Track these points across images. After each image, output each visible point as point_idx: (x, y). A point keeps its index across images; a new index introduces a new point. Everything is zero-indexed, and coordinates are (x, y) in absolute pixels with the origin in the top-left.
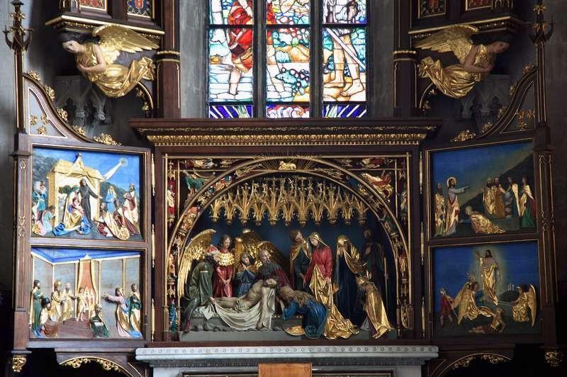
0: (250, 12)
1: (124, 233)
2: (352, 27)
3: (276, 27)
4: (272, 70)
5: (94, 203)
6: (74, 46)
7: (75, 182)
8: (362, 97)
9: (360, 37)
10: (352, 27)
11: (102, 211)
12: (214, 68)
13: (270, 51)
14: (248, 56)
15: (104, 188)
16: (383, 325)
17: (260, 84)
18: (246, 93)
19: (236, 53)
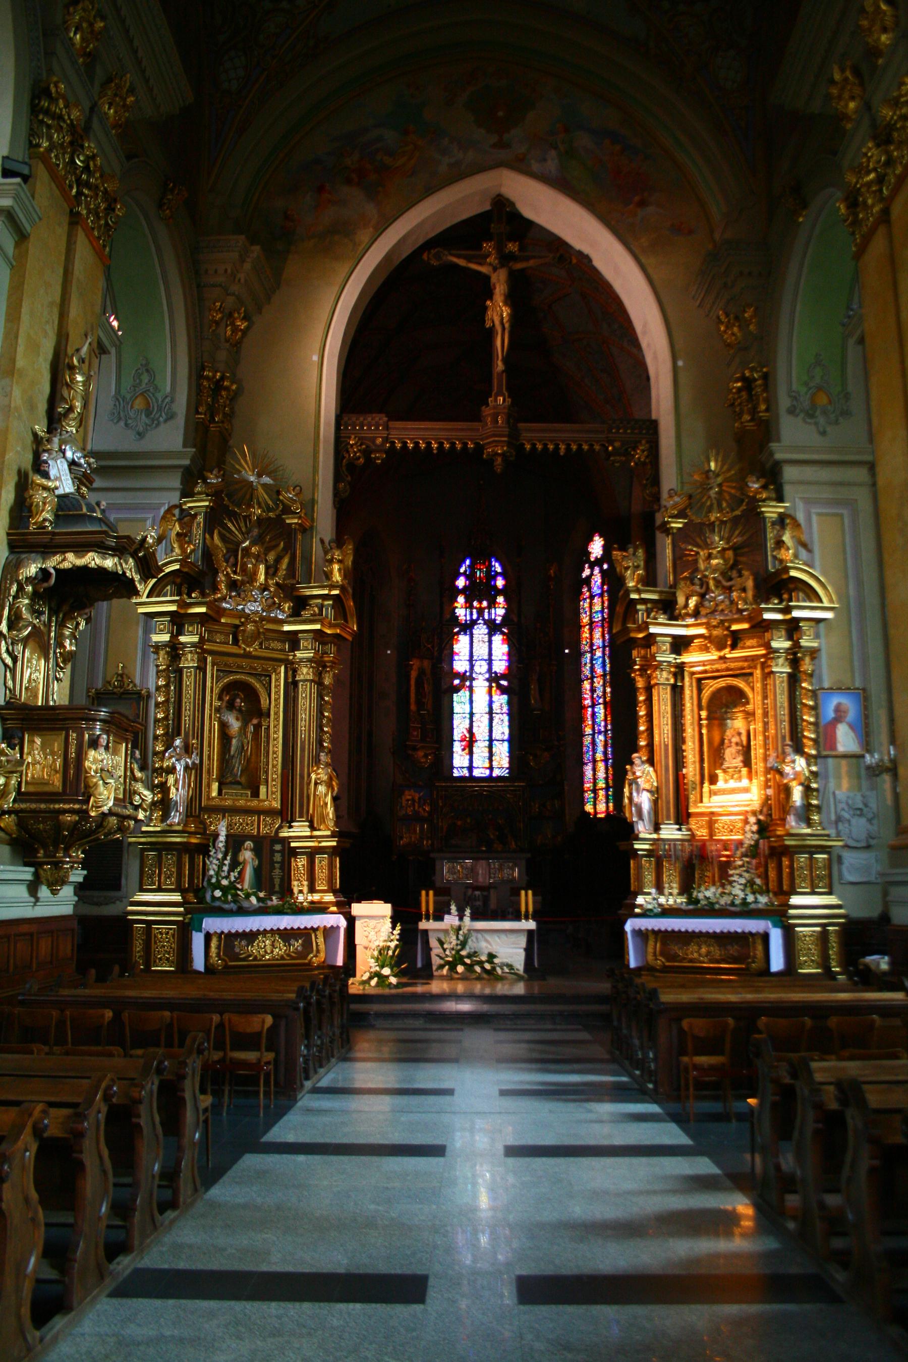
0: (467, 735)
1: (426, 814)
2: (503, 741)
5: (416, 805)
6: (410, 752)
7: (409, 797)
8: (507, 765)
9: (506, 744)
10: (503, 741)
11: (419, 807)
13: (474, 749)
14: (467, 751)
15: (419, 798)
16: (513, 845)
18: (466, 764)
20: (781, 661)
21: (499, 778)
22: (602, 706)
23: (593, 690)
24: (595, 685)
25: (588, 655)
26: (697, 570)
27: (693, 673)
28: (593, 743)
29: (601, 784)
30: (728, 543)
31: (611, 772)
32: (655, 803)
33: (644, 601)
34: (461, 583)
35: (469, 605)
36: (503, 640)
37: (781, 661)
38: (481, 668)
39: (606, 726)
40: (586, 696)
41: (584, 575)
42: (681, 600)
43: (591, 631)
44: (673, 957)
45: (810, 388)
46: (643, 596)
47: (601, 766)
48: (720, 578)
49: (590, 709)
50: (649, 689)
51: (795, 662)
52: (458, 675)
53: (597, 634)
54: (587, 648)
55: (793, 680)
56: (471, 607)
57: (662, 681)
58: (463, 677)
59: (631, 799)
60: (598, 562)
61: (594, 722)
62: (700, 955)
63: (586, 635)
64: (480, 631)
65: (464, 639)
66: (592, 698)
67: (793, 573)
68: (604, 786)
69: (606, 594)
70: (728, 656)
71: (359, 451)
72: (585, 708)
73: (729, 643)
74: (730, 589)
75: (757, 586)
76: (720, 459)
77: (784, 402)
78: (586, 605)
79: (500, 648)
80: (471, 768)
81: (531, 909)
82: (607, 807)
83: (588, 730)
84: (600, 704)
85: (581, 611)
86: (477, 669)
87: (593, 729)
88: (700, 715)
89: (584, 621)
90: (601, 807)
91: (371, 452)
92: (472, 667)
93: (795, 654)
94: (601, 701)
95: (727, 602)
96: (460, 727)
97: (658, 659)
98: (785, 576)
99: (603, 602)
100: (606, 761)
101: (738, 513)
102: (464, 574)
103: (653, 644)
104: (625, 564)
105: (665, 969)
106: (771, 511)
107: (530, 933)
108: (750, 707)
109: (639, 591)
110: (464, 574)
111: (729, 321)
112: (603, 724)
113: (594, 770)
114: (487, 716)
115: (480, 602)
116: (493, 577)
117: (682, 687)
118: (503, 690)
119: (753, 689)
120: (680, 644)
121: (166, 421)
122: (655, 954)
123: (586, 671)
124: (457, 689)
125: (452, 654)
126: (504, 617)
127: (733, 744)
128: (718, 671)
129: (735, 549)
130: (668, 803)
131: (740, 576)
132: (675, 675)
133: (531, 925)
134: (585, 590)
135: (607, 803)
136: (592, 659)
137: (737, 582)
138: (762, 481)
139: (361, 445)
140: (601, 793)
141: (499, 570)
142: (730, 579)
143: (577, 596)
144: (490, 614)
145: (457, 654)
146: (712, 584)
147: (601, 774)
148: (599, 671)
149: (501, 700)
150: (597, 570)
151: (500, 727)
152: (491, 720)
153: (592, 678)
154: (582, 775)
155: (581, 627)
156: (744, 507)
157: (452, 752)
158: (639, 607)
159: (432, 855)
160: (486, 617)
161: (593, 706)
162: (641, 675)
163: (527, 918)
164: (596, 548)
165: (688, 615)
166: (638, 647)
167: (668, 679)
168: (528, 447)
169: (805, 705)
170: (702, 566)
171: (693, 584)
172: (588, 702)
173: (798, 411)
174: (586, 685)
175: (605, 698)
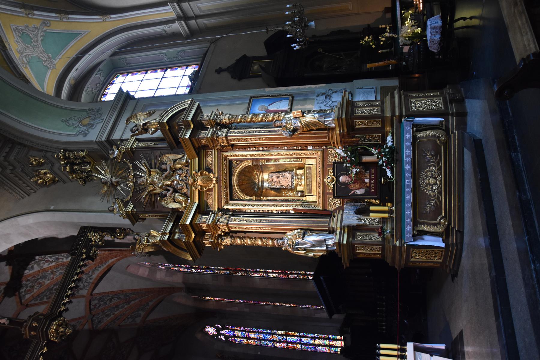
22: (288, 337)
23: (279, 341)
24: (277, 340)
25: (262, 342)
28: (306, 344)
29: (327, 342)
31: (320, 336)
32: (311, 231)
33: (172, 233)
37: (220, 133)
39: (297, 336)
40: (282, 346)
41: (224, 339)
43: (250, 339)
44: (438, 208)
45: (78, 125)
46: (168, 232)
47: (318, 342)
49: (289, 345)
53: (253, 335)
54: (259, 342)
57: (225, 221)
59: (307, 250)
60: (218, 330)
62: (435, 184)
63: (252, 342)
66: (283, 342)
68: (328, 341)
69: (233, 328)
70: (216, 176)
72: (288, 347)
73: (207, 173)
77: (80, 138)
78: (238, 339)
81: (395, 346)
82: (339, 340)
83: (299, 346)
84: (286, 338)
85: (241, 343)
89: (246, 342)
90: (339, 344)
94: (285, 337)
97: (210, 223)
99: (237, 330)
100: (315, 338)
101: (131, 165)
104: (144, 241)
105: (447, 216)
107: (416, 349)
109: (164, 234)
111: (37, 175)
112: (297, 338)
113: (319, 345)
119: (241, 161)
122: (435, 225)
123: (270, 344)
127: (278, 180)
128: (226, 185)
129: (150, 167)
130: (314, 222)
133: (410, 346)
134: (231, 340)
135: (337, 340)
136: (264, 340)
137: (169, 164)
138: (114, 148)
140: (332, 343)
143: (233, 344)
146: (169, 182)
147: (322, 342)
148: (270, 337)
150: (222, 332)
153: (273, 341)
154: (321, 353)
155: (248, 344)
156: (128, 162)
158: (176, 237)
161: (287, 342)
162: (222, 240)
163: (404, 350)
164: (211, 330)
165: (186, 201)
166: (202, 240)
167: (225, 218)
172: (285, 345)
173: (87, 132)
174: (277, 345)
175: (284, 335)
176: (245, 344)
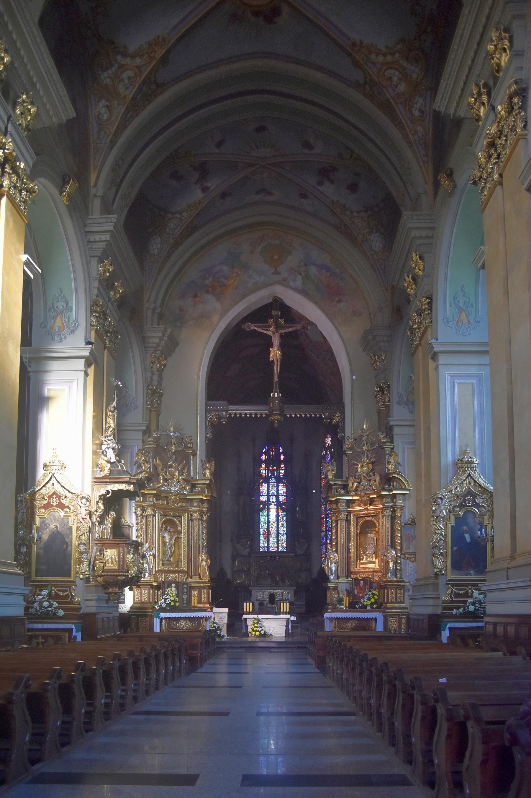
2: (284, 534)
3: (271, 534)
4: (270, 541)
8: (285, 546)
9: (285, 536)
10: (284, 534)
12: (261, 541)
13: (270, 538)
14: (266, 539)
17: (268, 544)
18: (266, 545)
19: (264, 539)
20: (388, 511)
21: (282, 552)
26: (357, 471)
27: (355, 515)
30: (370, 461)
33: (336, 485)
34: (263, 457)
35: (267, 468)
36: (283, 486)
38: (273, 499)
42: (350, 484)
46: (335, 483)
48: (366, 476)
50: (337, 521)
51: (394, 511)
52: (262, 503)
55: (393, 518)
56: (268, 469)
58: (264, 503)
60: (329, 448)
61: (326, 526)
64: (272, 482)
65: (265, 485)
66: (326, 515)
67: (394, 475)
70: (368, 508)
71: (216, 418)
72: (322, 519)
74: (370, 480)
75: (381, 479)
76: (368, 424)
79: (282, 490)
80: (268, 547)
86: (271, 500)
87: (326, 529)
88: (357, 532)
91: (221, 419)
92: (269, 499)
93: (394, 508)
95: (368, 486)
96: (263, 527)
98: (391, 476)
102: (265, 453)
103: (339, 503)
106: (388, 447)
108: (377, 529)
109: (333, 481)
110: (265, 453)
114: (276, 522)
115: (273, 467)
116: (280, 454)
117: (350, 520)
118: (283, 510)
119: (378, 522)
120: (349, 503)
121: (134, 409)
124: (262, 510)
125: (259, 493)
126: (284, 474)
131: (374, 475)
132: (347, 516)
137: (373, 478)
139: (216, 416)
141: (281, 450)
142: (370, 476)
143: (320, 464)
144: (277, 473)
145: (262, 493)
149: (282, 514)
151: (282, 528)
152: (278, 524)
157: (260, 540)
158: (333, 487)
159: (250, 588)
160: (276, 474)
165: (353, 491)
167: (344, 517)
168: (288, 415)
169: (398, 529)
170: (359, 470)
171: (355, 478)
176: (321, 476)
